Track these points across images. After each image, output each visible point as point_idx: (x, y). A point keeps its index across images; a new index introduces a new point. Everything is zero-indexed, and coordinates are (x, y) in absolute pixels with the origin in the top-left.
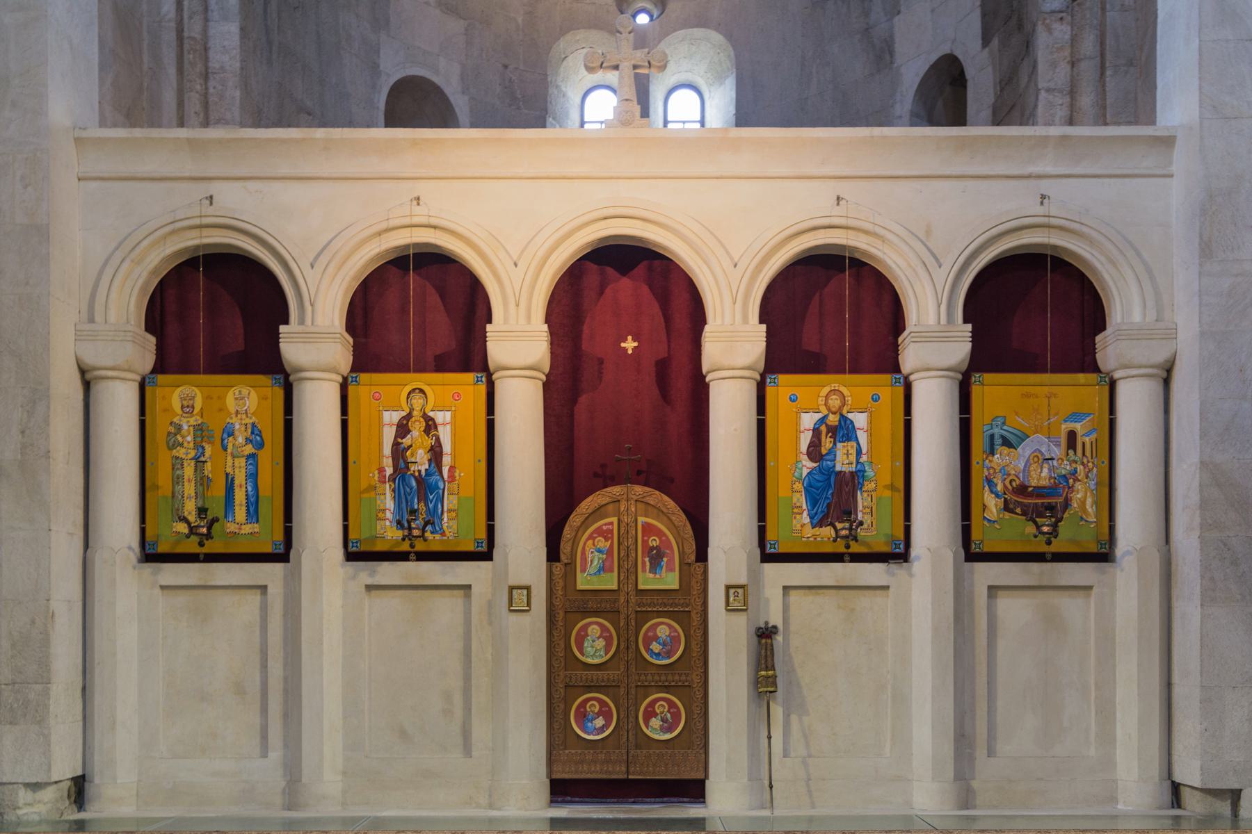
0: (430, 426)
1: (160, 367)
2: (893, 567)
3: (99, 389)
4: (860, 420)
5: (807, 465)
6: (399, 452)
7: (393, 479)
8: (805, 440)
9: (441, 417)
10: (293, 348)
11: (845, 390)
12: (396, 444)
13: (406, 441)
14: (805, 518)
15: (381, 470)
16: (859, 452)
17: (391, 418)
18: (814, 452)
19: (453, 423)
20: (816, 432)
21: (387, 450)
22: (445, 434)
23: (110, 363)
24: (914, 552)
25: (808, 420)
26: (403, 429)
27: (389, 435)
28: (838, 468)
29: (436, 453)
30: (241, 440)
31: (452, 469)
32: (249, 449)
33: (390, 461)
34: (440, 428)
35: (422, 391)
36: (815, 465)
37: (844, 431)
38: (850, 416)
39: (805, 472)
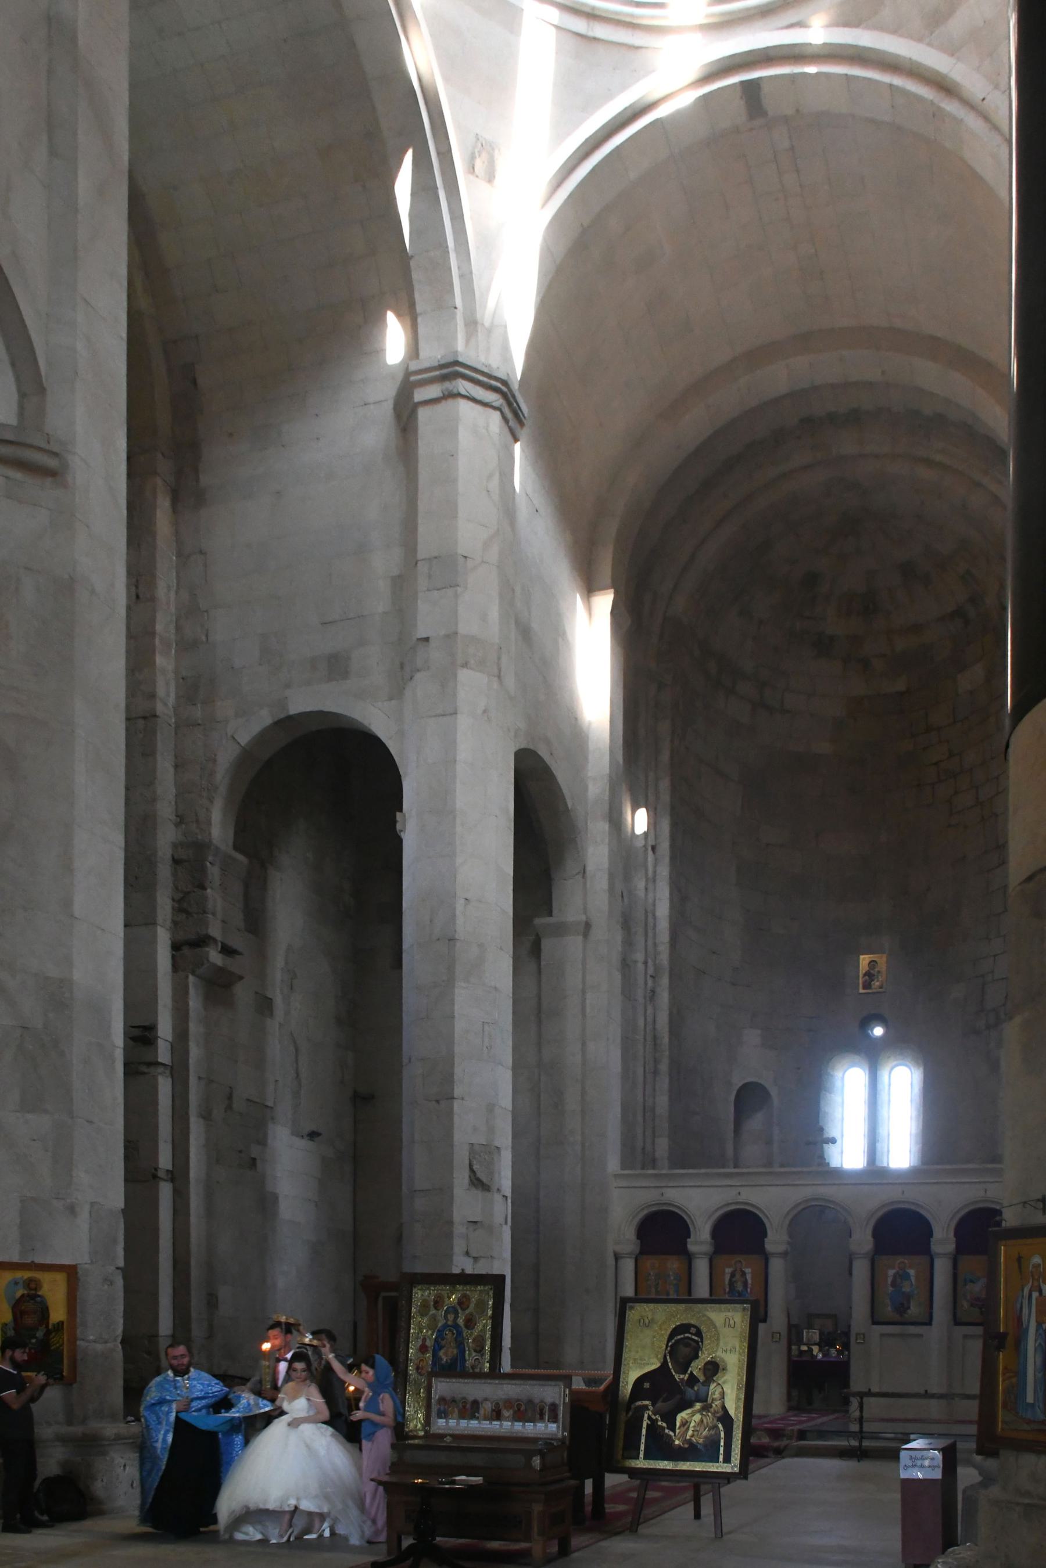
0: (744, 1274)
1: (642, 1252)
2: (925, 1327)
3: (621, 1262)
4: (912, 1272)
5: (891, 1289)
6: (731, 1284)
7: (729, 1293)
8: (890, 1280)
9: (748, 1271)
10: (692, 1248)
11: (906, 1261)
12: (730, 1280)
13: (734, 1279)
14: (889, 1309)
15: (725, 1290)
16: (912, 1285)
17: (728, 1270)
18: (893, 1284)
19: (752, 1273)
20: (895, 1276)
21: (727, 1282)
22: (749, 1277)
23: (625, 1252)
24: (934, 1322)
25: (891, 1272)
26: (733, 1275)
27: (727, 1278)
28: (904, 1290)
29: (745, 1283)
30: (672, 1278)
31: (751, 1290)
32: (675, 1282)
33: (728, 1286)
34: (747, 1275)
35: (740, 1261)
36: (893, 1289)
37: (905, 1276)
38: (908, 1271)
39: (890, 1292)
